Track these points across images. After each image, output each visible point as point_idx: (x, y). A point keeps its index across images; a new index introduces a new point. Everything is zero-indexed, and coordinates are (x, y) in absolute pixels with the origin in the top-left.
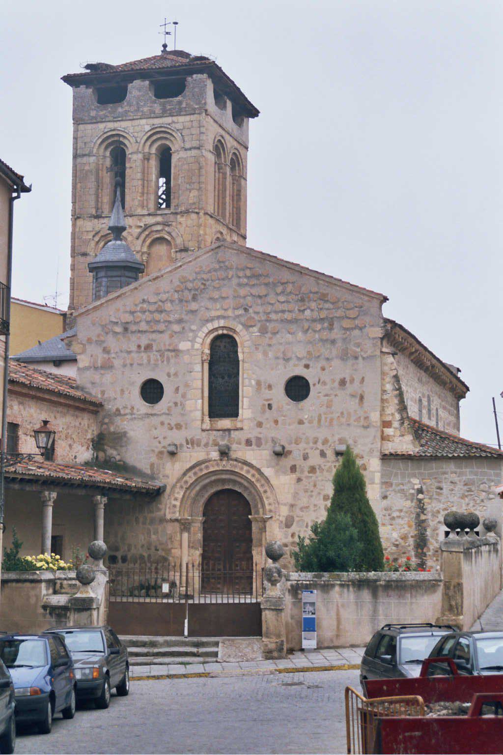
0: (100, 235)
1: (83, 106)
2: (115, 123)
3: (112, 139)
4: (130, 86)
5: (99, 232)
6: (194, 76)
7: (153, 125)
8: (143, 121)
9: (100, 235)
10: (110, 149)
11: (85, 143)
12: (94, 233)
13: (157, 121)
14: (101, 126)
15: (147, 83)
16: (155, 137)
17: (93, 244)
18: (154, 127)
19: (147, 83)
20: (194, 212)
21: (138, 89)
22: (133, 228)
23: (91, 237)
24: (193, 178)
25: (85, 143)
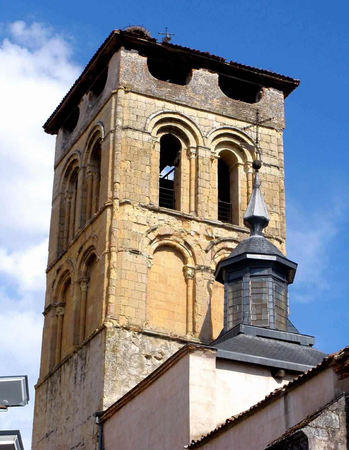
0: (156, 233)
1: (135, 73)
2: (177, 106)
3: (173, 124)
4: (195, 71)
5: (155, 229)
6: (272, 90)
7: (225, 124)
8: (212, 116)
9: (156, 233)
10: (161, 135)
11: (137, 116)
12: (147, 228)
13: (230, 122)
14: (160, 104)
15: (216, 76)
16: (222, 139)
17: (146, 241)
18: (225, 126)
19: (216, 76)
20: (277, 239)
21: (204, 79)
22: (201, 236)
23: (143, 232)
24: (274, 199)
25: (137, 116)
